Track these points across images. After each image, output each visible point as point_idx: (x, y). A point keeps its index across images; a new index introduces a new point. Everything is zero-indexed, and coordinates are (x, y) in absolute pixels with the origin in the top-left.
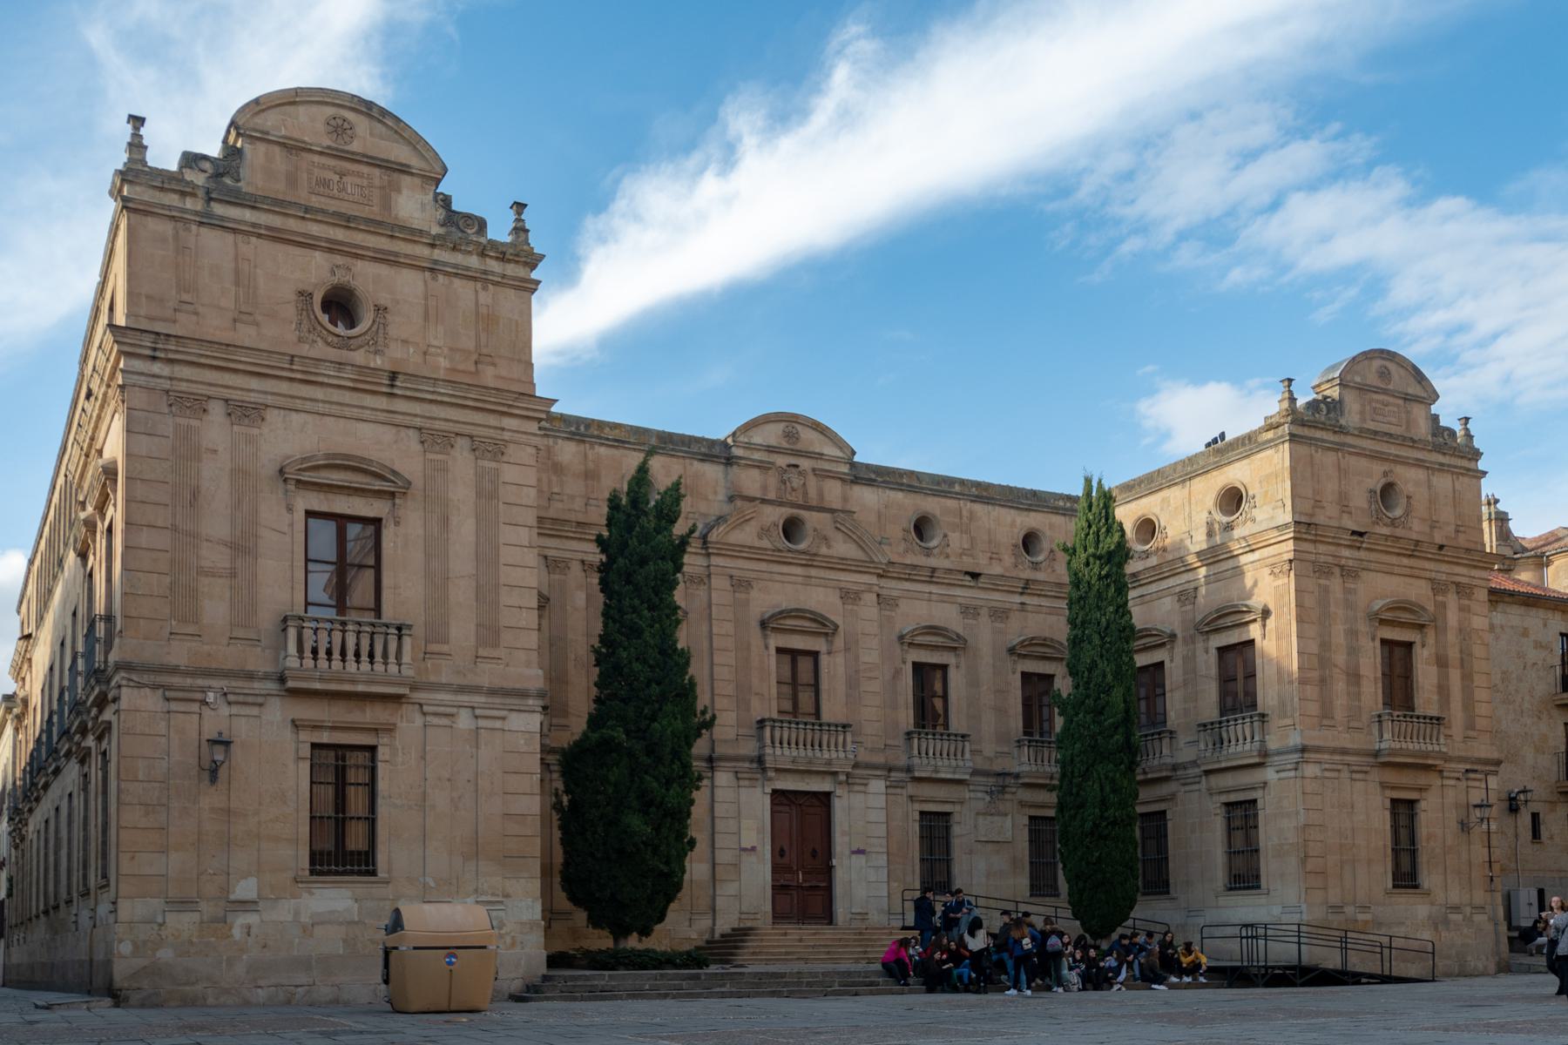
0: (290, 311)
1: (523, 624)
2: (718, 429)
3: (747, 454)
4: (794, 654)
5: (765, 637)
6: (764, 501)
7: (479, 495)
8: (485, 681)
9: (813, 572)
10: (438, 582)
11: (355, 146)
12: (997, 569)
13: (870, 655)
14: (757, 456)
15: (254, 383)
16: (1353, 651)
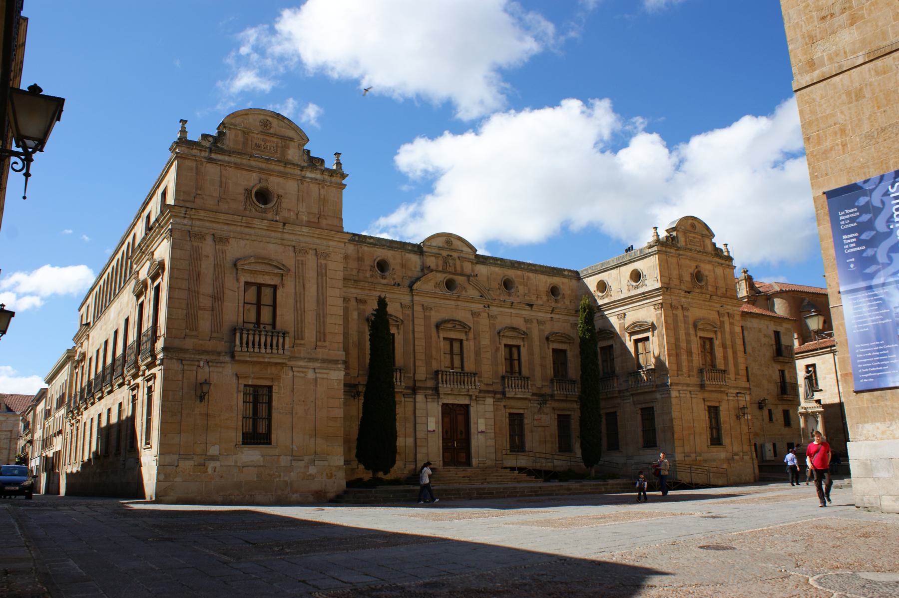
0: (242, 198)
1: (336, 331)
2: (417, 241)
3: (429, 250)
4: (451, 341)
5: (438, 332)
6: (437, 271)
7: (318, 275)
8: (320, 356)
9: (459, 303)
11: (272, 131)
12: (540, 302)
13: (485, 341)
14: (434, 251)
15: (226, 227)
16: (688, 342)
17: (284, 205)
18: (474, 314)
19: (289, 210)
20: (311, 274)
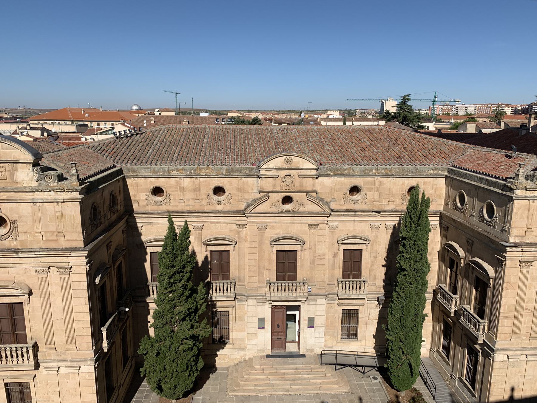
7: (62, 288)
17: (19, 229)
18: (310, 227)
19: (25, 232)
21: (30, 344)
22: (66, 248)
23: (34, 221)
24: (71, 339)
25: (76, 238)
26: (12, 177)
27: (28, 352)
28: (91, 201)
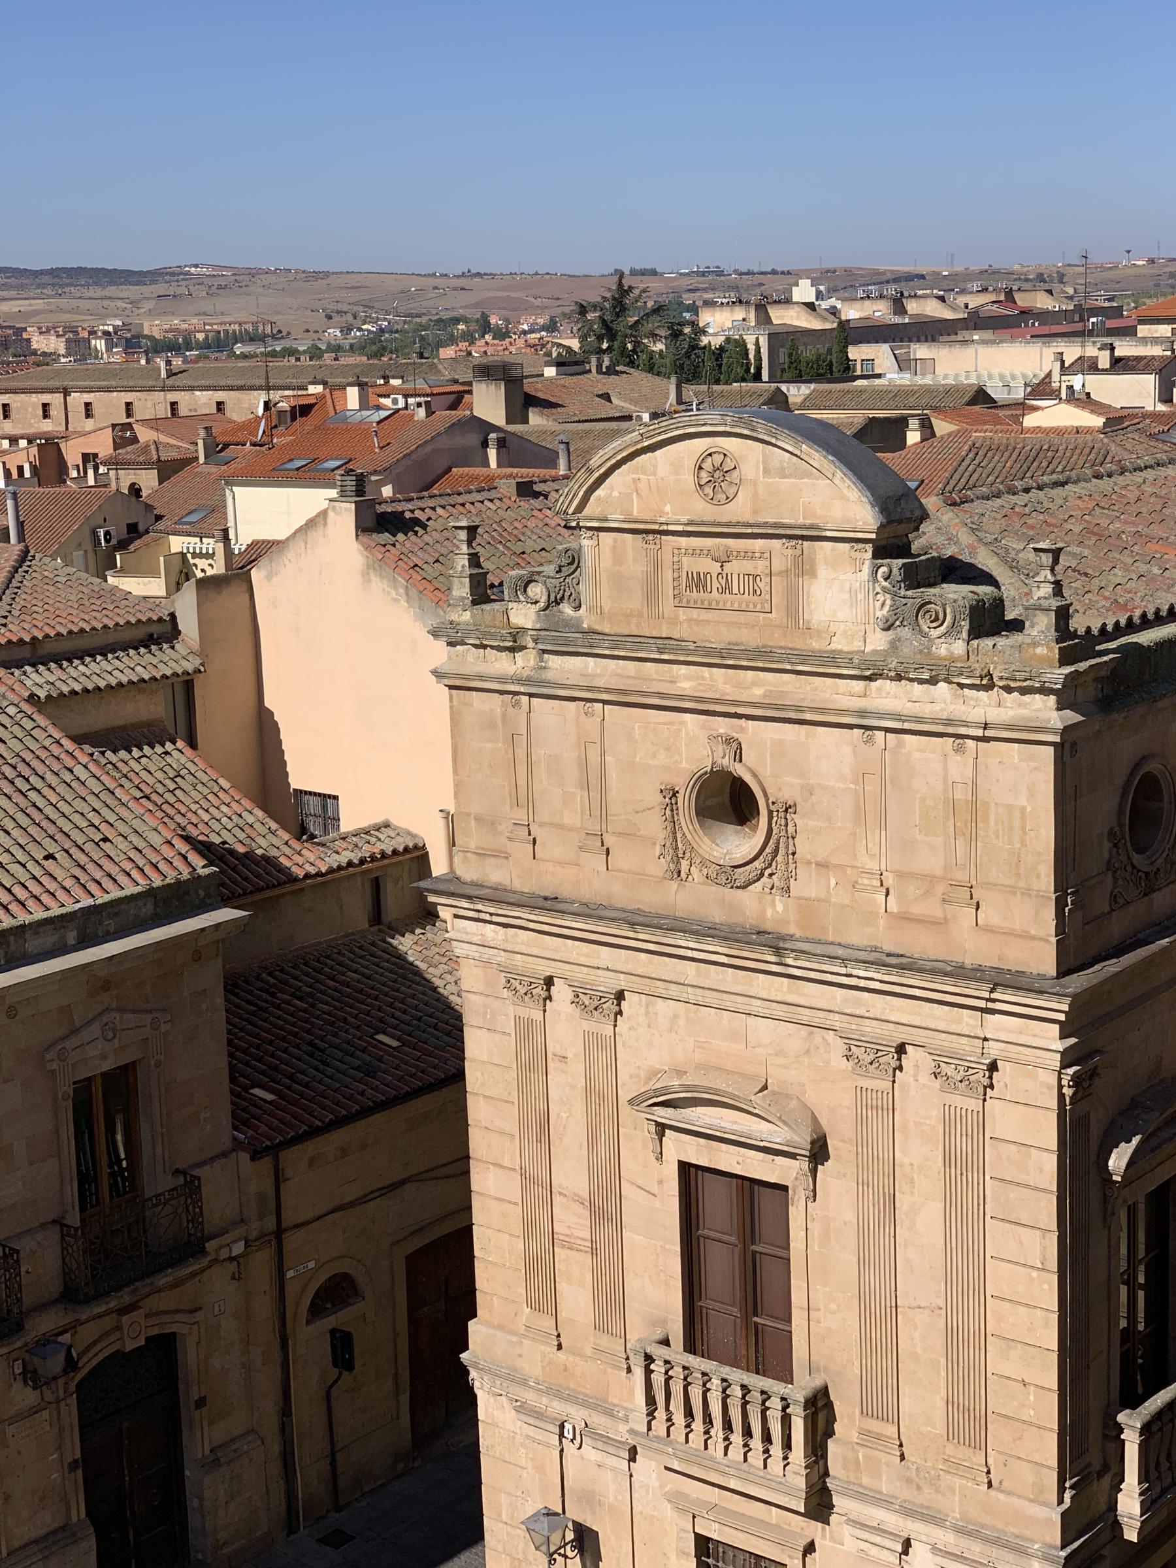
1: (1029, 1414)
10: (881, 1315)
17: (803, 846)
19: (823, 865)
20: (919, 1157)
21: (798, 1392)
22: (979, 969)
23: (859, 815)
24: (970, 1423)
25: (1023, 924)
26: (794, 605)
27: (786, 1420)
28: (1128, 748)
